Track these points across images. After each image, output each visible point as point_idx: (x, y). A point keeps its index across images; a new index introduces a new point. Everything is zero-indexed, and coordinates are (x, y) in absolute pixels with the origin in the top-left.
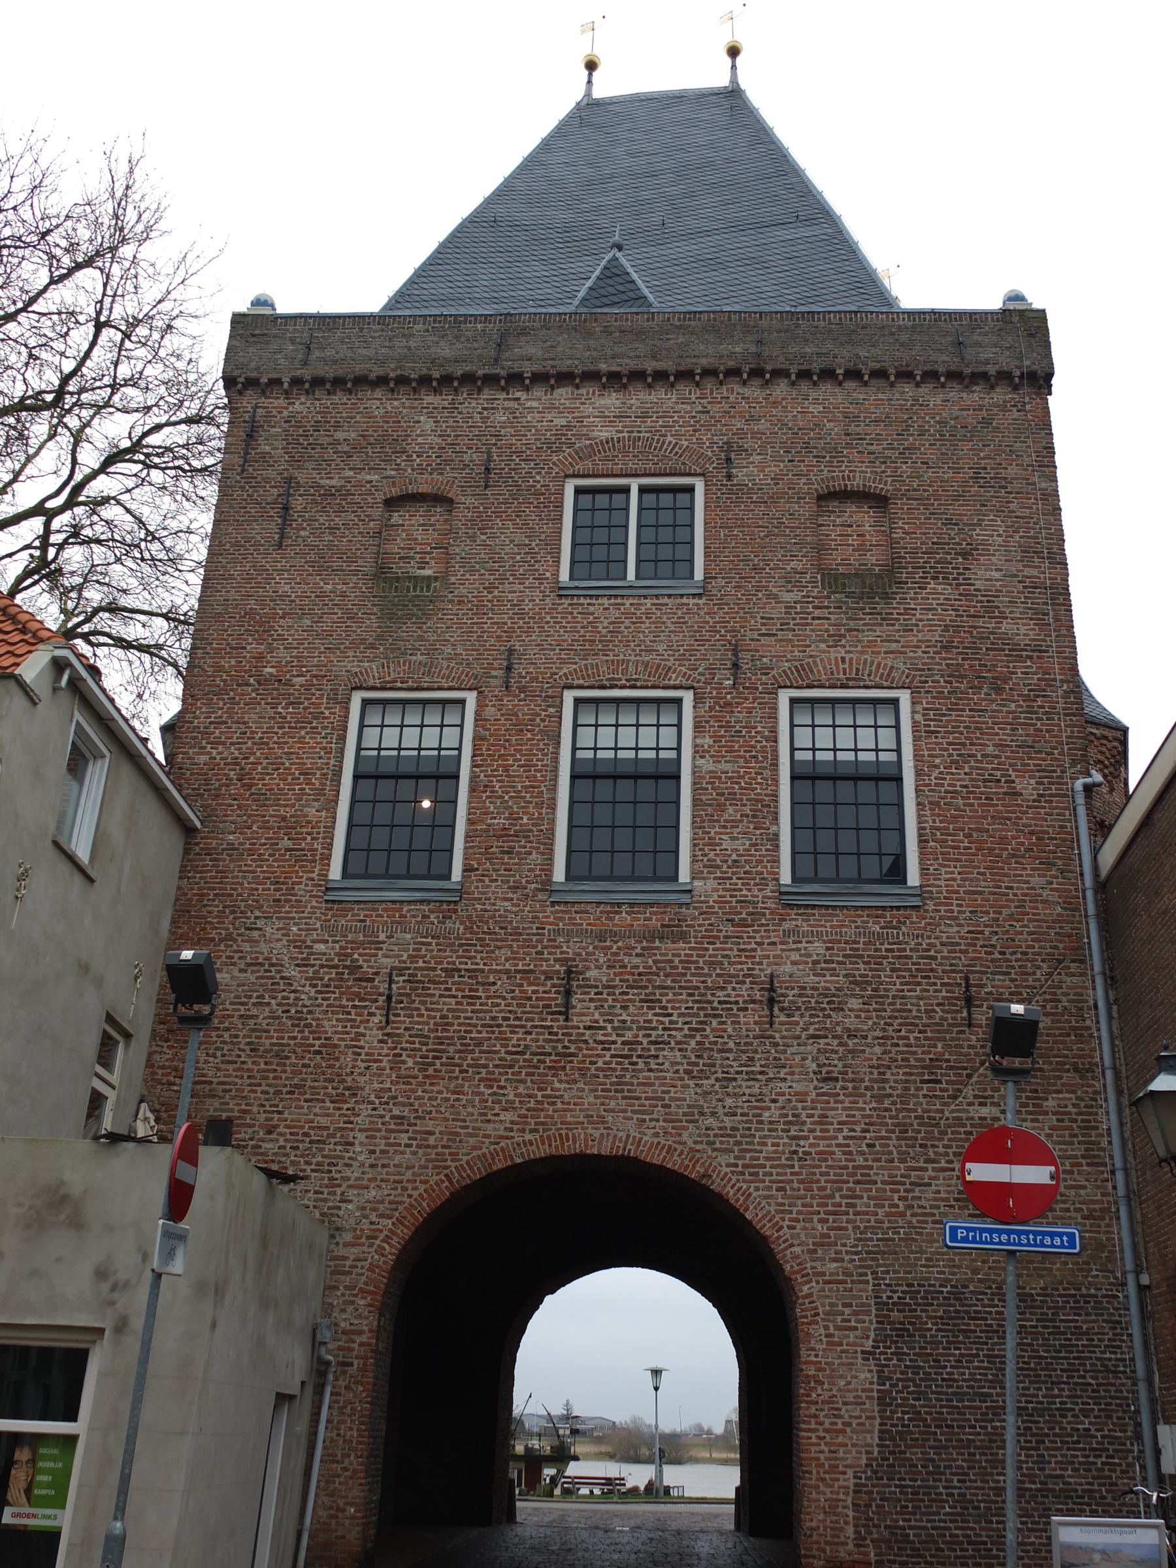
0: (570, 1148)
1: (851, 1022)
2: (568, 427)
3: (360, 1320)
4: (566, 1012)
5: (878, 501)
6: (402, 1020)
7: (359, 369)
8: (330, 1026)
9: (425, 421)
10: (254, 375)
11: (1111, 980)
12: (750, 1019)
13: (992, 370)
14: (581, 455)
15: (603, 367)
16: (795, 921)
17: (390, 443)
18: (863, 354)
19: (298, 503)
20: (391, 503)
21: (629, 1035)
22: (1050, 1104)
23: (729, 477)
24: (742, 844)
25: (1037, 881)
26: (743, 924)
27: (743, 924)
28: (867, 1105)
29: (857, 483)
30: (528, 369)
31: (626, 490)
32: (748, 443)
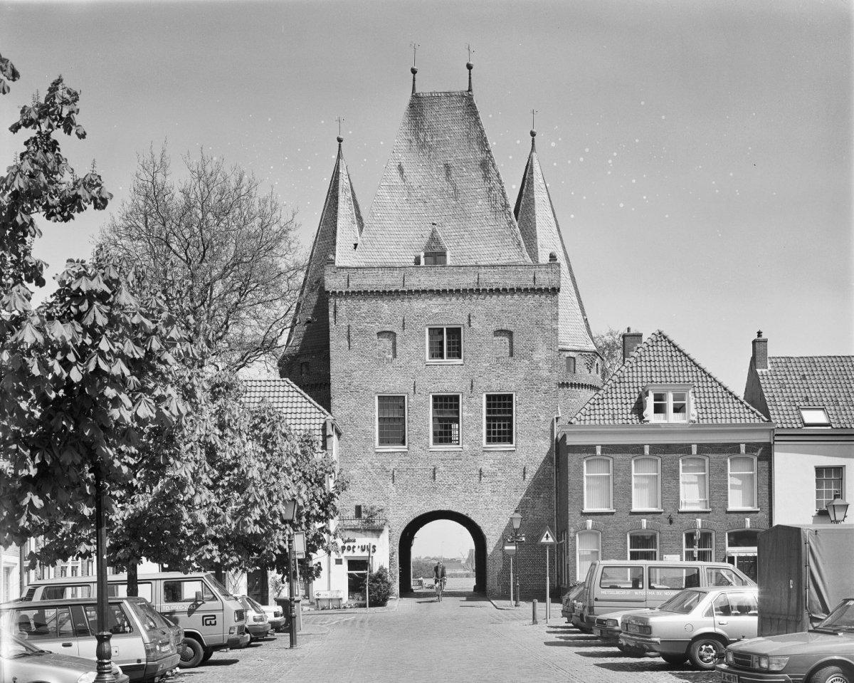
0: (436, 509)
1: (499, 479)
2: (426, 308)
3: (397, 549)
4: (434, 478)
5: (510, 334)
6: (397, 481)
7: (365, 288)
8: (381, 482)
9: (385, 306)
10: (334, 290)
11: (557, 466)
12: (477, 478)
13: (543, 287)
14: (430, 318)
15: (435, 289)
16: (486, 454)
17: (376, 315)
18: (508, 282)
19: (352, 335)
20: (379, 334)
21: (449, 483)
22: (542, 496)
23: (470, 326)
24: (474, 435)
25: (542, 442)
26: (475, 455)
27: (475, 455)
28: (501, 497)
29: (504, 328)
30: (414, 289)
31: (443, 329)
32: (475, 314)
